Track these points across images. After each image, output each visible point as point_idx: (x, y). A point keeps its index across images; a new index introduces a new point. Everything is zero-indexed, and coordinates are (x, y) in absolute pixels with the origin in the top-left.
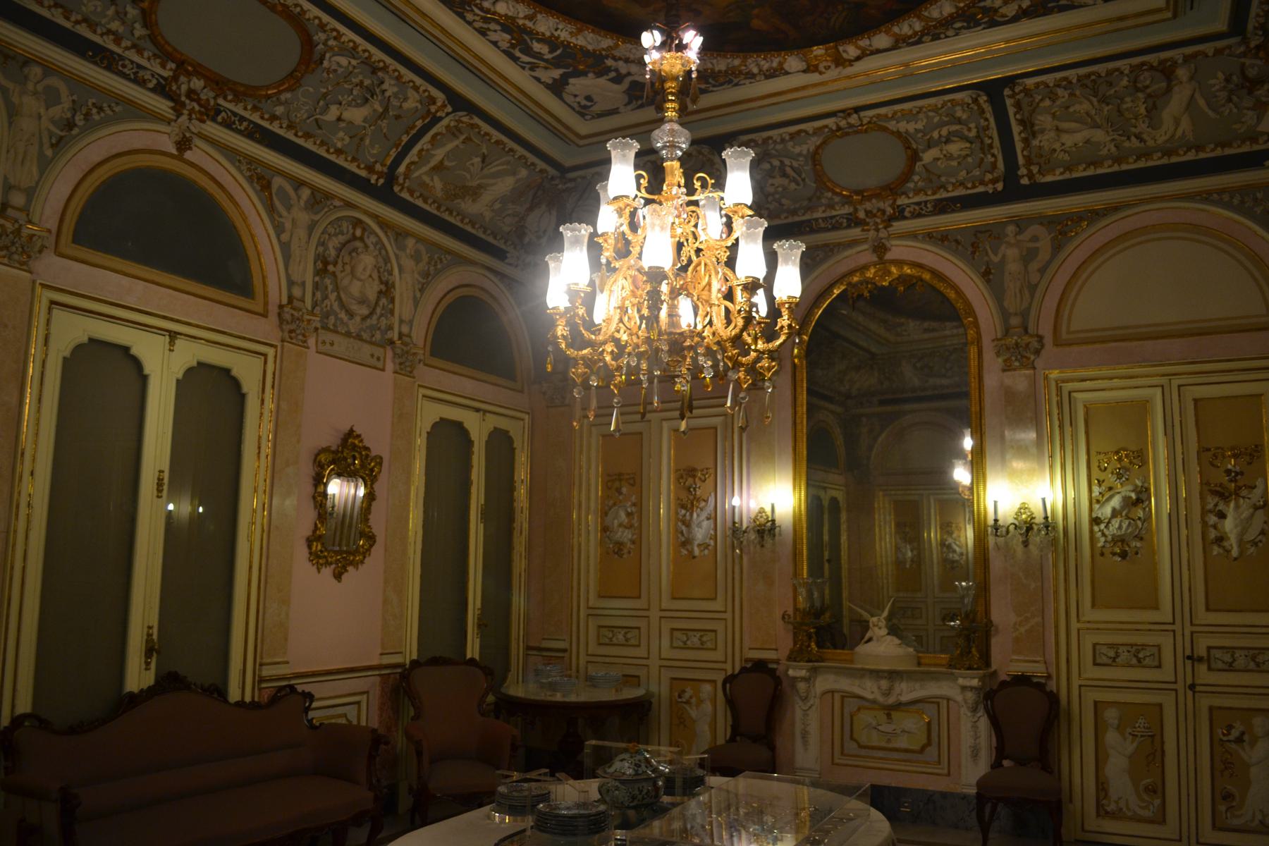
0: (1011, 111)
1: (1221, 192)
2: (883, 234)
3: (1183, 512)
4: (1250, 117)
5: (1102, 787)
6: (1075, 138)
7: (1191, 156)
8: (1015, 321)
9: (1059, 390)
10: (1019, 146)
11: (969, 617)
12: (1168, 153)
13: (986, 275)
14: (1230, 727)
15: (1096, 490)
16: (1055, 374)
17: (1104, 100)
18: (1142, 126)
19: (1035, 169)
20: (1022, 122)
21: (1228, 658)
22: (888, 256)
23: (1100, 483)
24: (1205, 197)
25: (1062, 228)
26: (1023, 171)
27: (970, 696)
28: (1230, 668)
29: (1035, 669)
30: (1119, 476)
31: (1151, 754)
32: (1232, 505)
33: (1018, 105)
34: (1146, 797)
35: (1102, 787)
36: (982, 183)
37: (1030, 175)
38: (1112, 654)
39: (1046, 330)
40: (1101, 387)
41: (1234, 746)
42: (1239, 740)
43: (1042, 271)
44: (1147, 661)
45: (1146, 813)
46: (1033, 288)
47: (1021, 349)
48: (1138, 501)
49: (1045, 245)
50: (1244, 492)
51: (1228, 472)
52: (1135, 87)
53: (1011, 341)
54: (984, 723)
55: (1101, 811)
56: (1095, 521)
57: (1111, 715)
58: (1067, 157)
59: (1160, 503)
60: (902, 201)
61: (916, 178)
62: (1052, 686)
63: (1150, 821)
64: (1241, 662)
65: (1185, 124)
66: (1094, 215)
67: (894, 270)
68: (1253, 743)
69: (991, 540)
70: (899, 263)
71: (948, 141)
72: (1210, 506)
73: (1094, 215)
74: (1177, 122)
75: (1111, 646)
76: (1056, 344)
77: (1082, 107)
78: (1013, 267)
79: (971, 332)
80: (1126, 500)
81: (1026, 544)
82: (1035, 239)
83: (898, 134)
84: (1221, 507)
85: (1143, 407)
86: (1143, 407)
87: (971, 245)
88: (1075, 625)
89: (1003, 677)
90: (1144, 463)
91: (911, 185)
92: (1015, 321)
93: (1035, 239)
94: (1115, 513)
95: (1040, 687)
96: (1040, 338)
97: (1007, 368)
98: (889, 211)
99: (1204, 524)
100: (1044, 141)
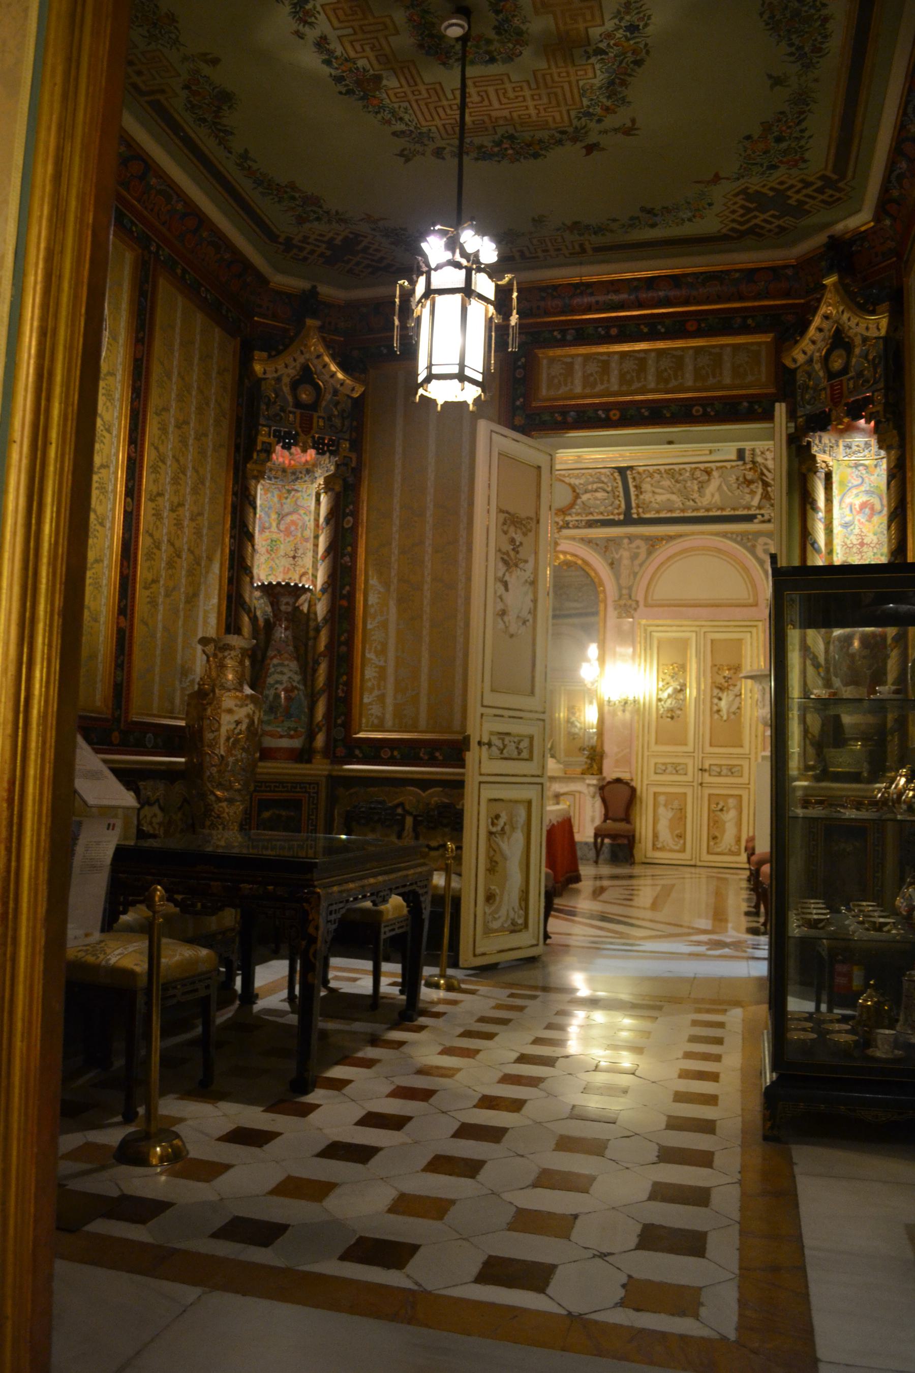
0: (630, 481)
1: (732, 533)
2: (557, 536)
3: (702, 697)
4: (748, 497)
5: (656, 836)
6: (662, 498)
7: (719, 513)
8: (625, 592)
9: (645, 630)
10: (633, 498)
11: (593, 749)
12: (708, 510)
13: (612, 564)
14: (717, 804)
15: (661, 684)
16: (644, 622)
17: (677, 481)
18: (696, 495)
19: (641, 510)
20: (636, 487)
21: (718, 770)
22: (559, 548)
23: (663, 680)
24: (725, 535)
25: (653, 543)
26: (634, 511)
27: (592, 789)
28: (719, 775)
29: (625, 776)
30: (673, 677)
31: (680, 817)
32: (725, 694)
33: (634, 479)
34: (676, 839)
35: (656, 836)
36: (612, 514)
37: (638, 514)
38: (664, 768)
39: (640, 598)
40: (667, 630)
41: (719, 813)
42: (721, 810)
43: (641, 565)
44: (681, 772)
45: (677, 848)
46: (635, 574)
47: (627, 607)
48: (681, 690)
49: (643, 551)
50: (731, 688)
51: (725, 677)
52: (693, 478)
53: (622, 602)
54: (598, 803)
55: (655, 848)
56: (659, 700)
57: (662, 799)
58: (657, 506)
59: (691, 693)
60: (568, 518)
61: (577, 507)
62: (633, 784)
63: (679, 851)
64: (724, 772)
65: (717, 497)
66: (670, 538)
67: (562, 557)
68: (728, 812)
69: (606, 708)
70: (565, 553)
71: (596, 491)
72: (715, 694)
73: (670, 538)
74: (713, 495)
75: (664, 764)
76: (646, 606)
77: (666, 483)
78: (626, 562)
79: (602, 596)
80: (675, 689)
81: (624, 711)
82: (638, 547)
83: (570, 484)
84: (720, 695)
85: (685, 643)
86: (685, 643)
87: (605, 547)
88: (646, 753)
89: (608, 779)
90: (685, 671)
91: (574, 510)
92: (625, 592)
93: (638, 547)
94: (669, 696)
95: (627, 784)
96: (637, 602)
97: (620, 617)
98: (561, 523)
99: (712, 703)
100: (647, 497)
